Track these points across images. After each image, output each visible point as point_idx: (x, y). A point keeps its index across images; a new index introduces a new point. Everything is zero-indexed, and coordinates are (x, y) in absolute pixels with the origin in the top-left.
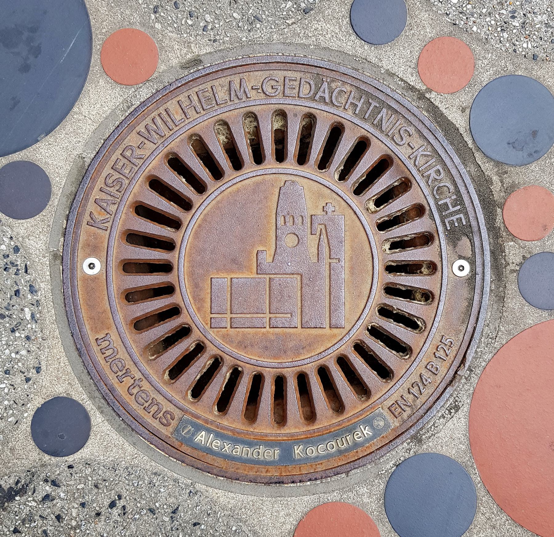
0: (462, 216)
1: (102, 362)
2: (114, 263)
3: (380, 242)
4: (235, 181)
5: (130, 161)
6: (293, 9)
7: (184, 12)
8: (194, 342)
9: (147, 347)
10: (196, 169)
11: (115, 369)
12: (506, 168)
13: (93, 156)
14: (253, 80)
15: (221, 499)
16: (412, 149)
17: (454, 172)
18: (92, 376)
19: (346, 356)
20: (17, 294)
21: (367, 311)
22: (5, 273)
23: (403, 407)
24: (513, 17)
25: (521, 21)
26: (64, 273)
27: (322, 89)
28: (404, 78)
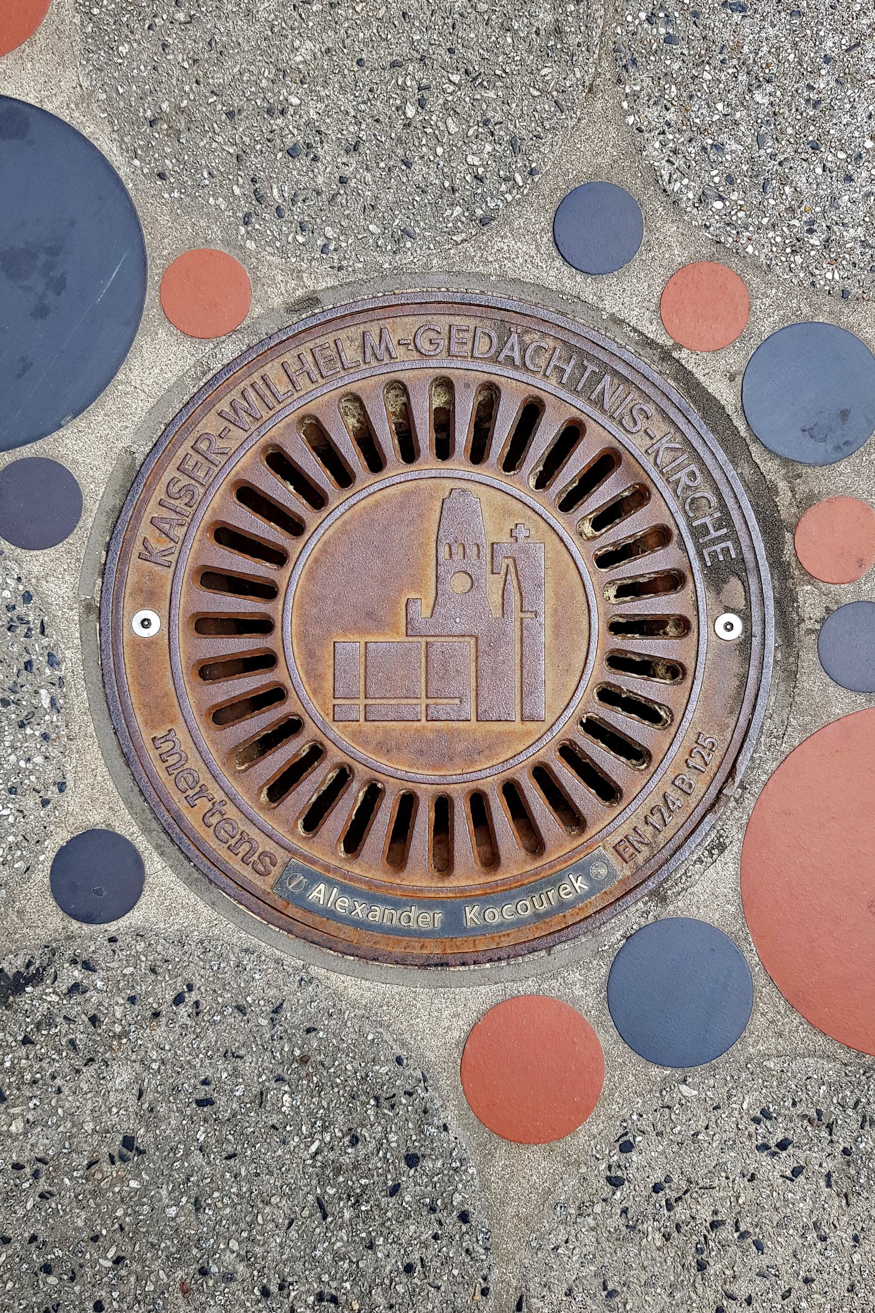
0: (729, 544)
1: (163, 775)
2: (181, 619)
3: (600, 587)
4: (371, 490)
5: (206, 458)
6: (464, 219)
7: (291, 222)
8: (307, 743)
9: (233, 751)
10: (312, 470)
11: (183, 785)
12: (800, 469)
13: (147, 450)
14: (400, 330)
15: (351, 991)
16: (652, 438)
17: (717, 475)
18: (147, 796)
19: (547, 766)
20: (29, 668)
21: (580, 694)
22: (9, 634)
23: (637, 845)
24: (811, 231)
25: (823, 236)
26: (103, 634)
27: (509, 345)
28: (639, 328)
